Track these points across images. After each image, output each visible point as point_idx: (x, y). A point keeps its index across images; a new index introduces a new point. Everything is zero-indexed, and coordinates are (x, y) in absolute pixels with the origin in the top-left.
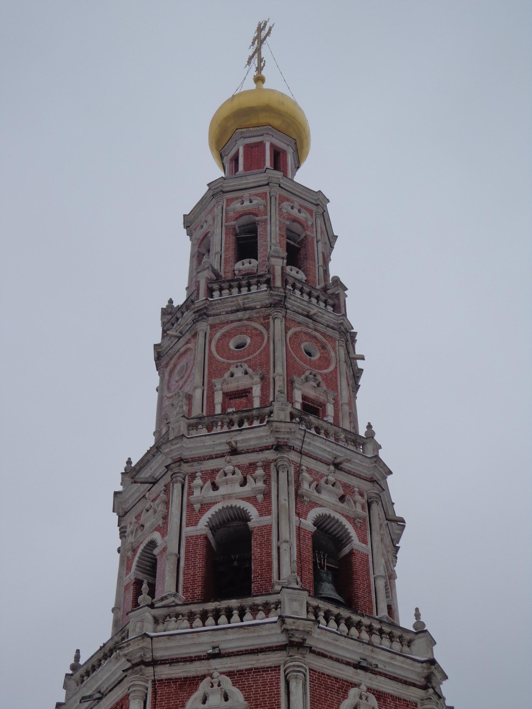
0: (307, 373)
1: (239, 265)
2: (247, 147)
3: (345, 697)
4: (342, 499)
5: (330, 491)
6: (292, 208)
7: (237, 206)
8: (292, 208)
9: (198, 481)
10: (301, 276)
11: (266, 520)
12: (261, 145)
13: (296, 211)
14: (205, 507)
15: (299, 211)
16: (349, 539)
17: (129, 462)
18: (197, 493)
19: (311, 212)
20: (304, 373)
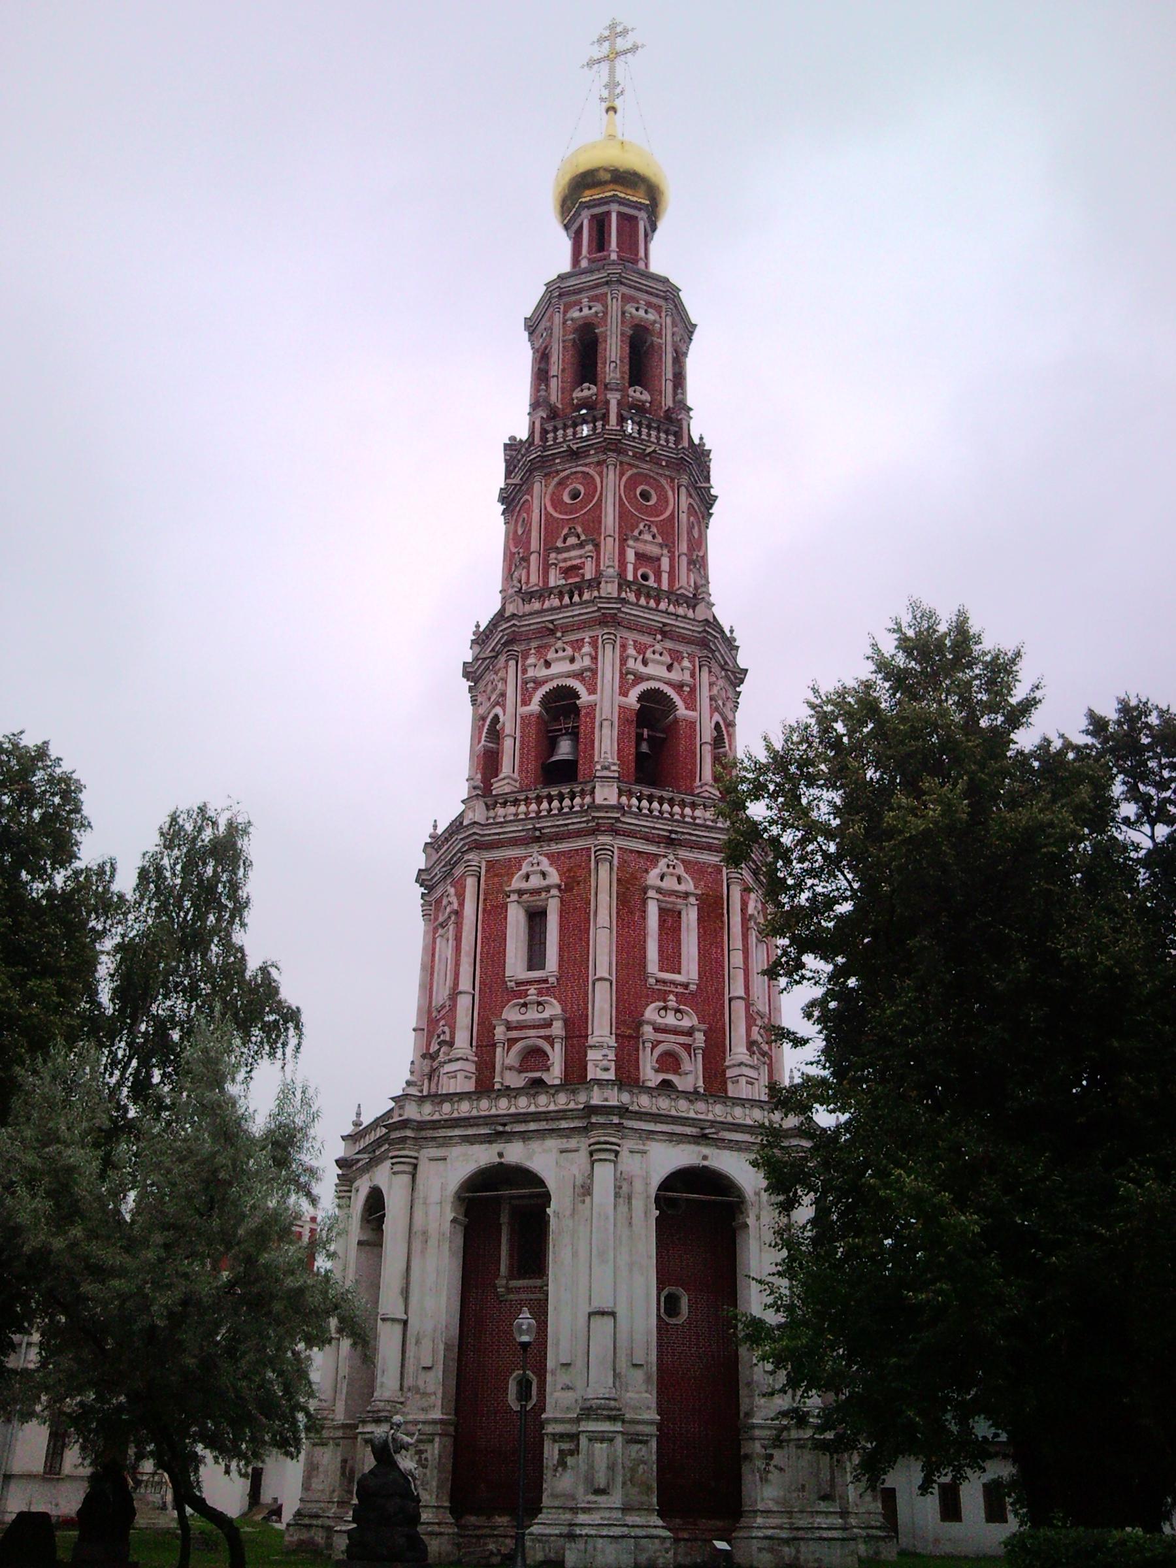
0: (641, 526)
1: (577, 394)
2: (593, 217)
3: (655, 866)
4: (670, 668)
5: (658, 662)
6: (637, 309)
8: (637, 309)
9: (531, 660)
10: (646, 397)
11: (592, 698)
12: (608, 213)
13: (641, 313)
14: (538, 683)
15: (646, 312)
16: (672, 706)
17: (478, 626)
18: (531, 673)
19: (658, 309)
20: (637, 527)
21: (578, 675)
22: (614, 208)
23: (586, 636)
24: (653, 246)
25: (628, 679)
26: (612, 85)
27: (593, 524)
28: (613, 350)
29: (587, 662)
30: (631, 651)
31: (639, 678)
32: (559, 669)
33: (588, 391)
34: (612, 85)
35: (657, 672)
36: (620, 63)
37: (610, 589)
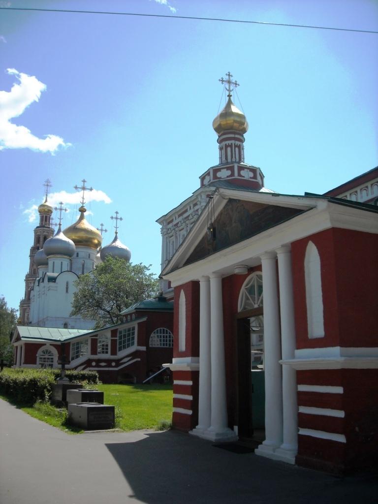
7: (38, 233)
12: (43, 216)
26: (47, 191)
28: (42, 239)
33: (38, 245)
36: (48, 187)
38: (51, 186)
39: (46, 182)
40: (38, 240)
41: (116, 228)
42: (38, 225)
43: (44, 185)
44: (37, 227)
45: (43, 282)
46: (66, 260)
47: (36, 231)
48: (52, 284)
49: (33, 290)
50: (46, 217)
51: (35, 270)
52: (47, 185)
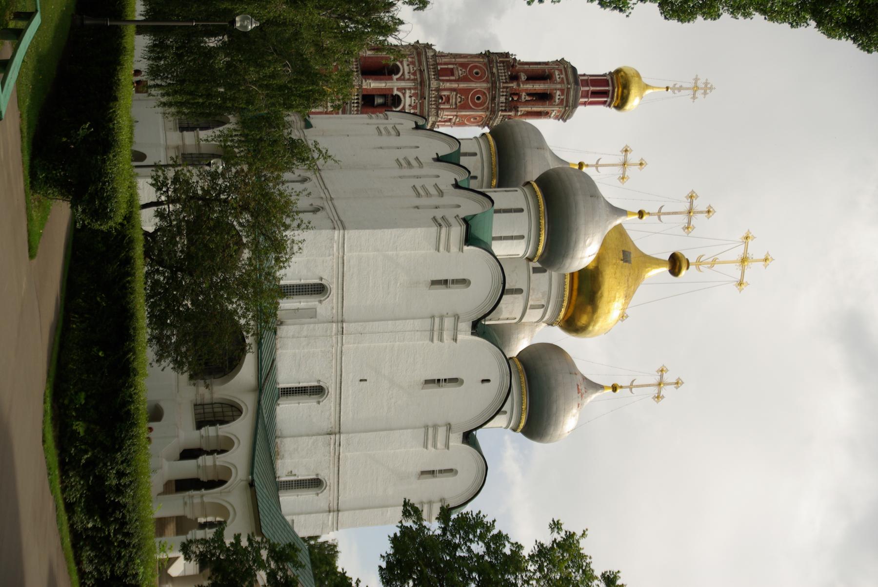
7: (557, 73)
12: (608, 85)
21: (403, 74)
22: (610, 88)
23: (418, 76)
24: (601, 108)
25: (403, 90)
26: (680, 89)
27: (465, 79)
28: (539, 87)
29: (407, 76)
30: (413, 91)
31: (404, 94)
32: (405, 67)
33: (523, 77)
34: (680, 89)
35: (407, 101)
37: (434, 84)
38: (694, 98)
39: (706, 84)
40: (540, 73)
41: (631, 387)
42: (579, 72)
43: (696, 80)
44: (574, 69)
45: (457, 186)
46: (526, 252)
47: (562, 65)
48: (457, 232)
49: (418, 127)
50: (604, 94)
51: (451, 72)
52: (695, 88)
